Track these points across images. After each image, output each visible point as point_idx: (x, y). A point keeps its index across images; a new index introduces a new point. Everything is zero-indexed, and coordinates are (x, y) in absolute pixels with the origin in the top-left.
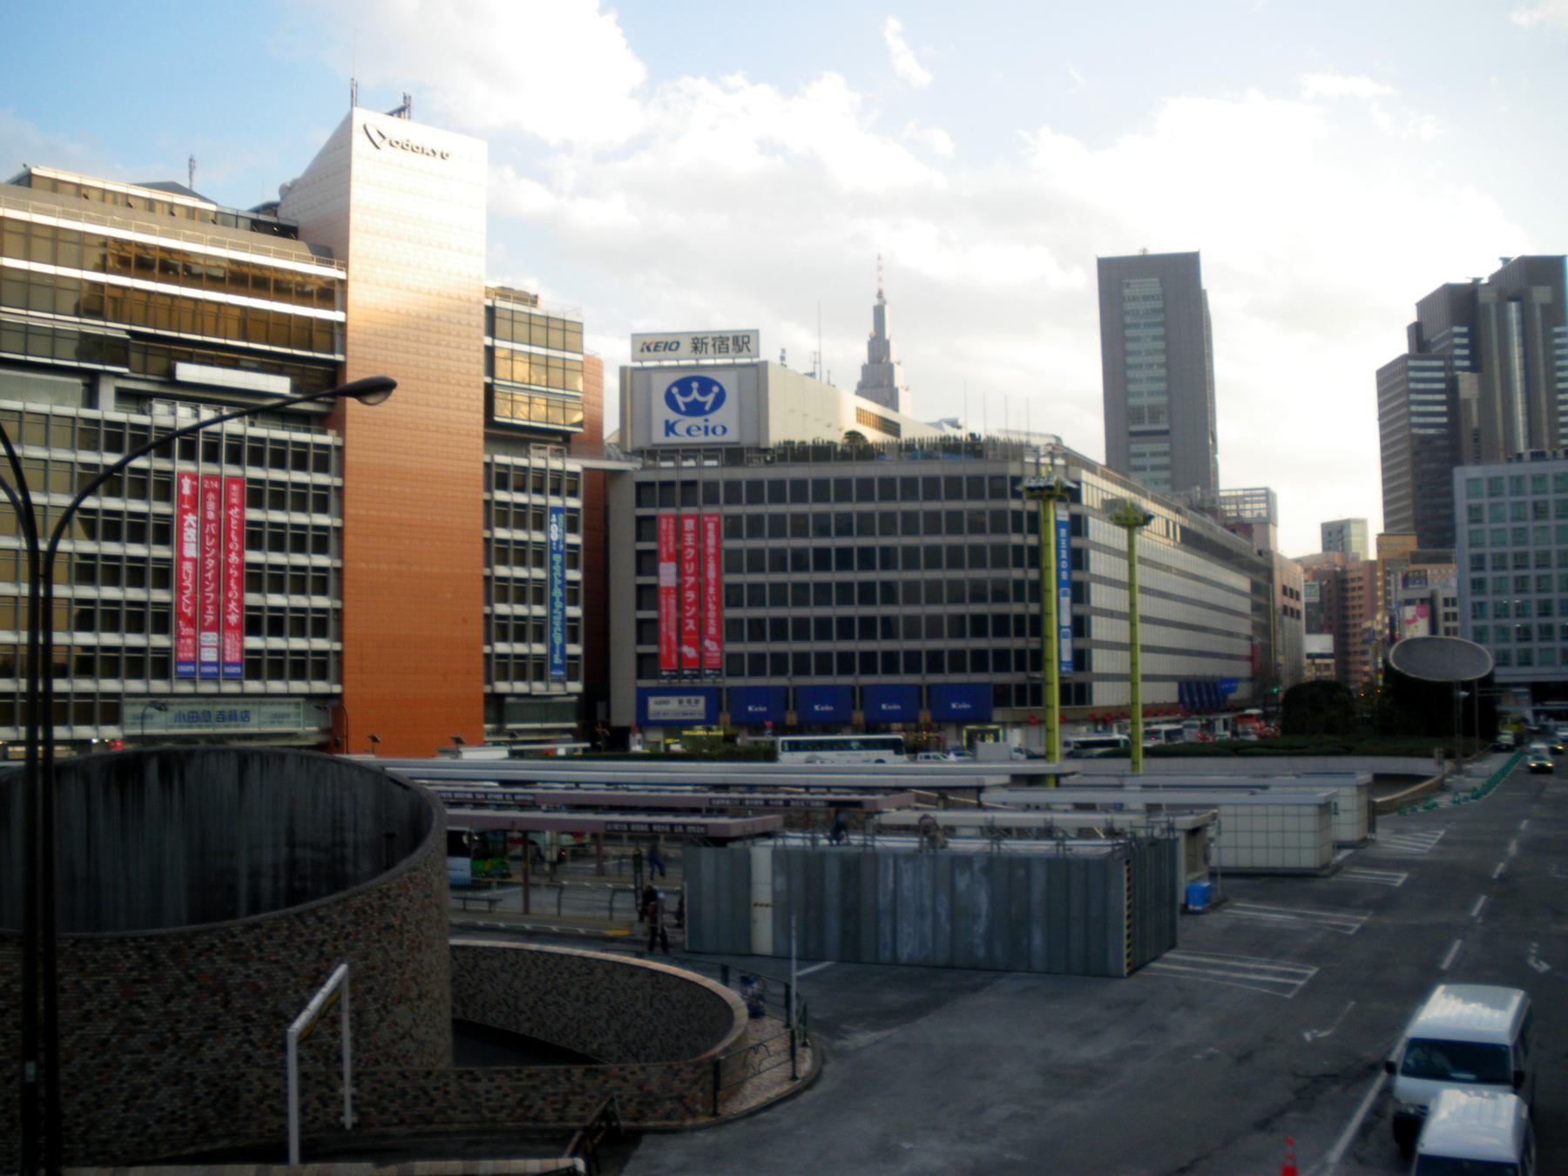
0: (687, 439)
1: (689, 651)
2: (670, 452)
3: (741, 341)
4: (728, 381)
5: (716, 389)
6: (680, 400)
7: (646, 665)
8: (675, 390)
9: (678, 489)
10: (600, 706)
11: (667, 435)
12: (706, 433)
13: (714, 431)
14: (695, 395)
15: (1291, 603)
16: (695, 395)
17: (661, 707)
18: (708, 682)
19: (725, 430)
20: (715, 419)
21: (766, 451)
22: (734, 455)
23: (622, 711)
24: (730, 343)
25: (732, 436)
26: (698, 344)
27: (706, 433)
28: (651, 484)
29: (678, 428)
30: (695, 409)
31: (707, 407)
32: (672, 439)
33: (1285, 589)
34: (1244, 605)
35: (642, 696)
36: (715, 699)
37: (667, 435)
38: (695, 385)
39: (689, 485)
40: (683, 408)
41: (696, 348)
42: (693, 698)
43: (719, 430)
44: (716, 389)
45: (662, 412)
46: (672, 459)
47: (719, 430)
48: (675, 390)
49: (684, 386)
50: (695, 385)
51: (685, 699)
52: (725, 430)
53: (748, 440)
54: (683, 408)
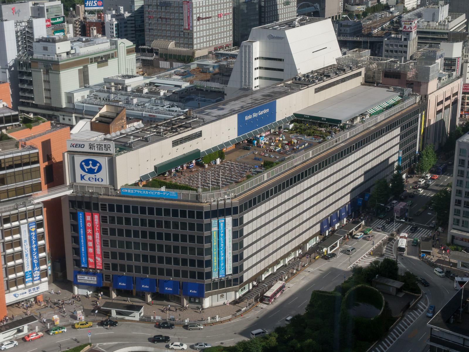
0: (89, 182)
2: (83, 187)
4: (103, 161)
5: (98, 165)
6: (86, 167)
8: (83, 163)
12: (96, 181)
13: (98, 180)
14: (91, 166)
16: (91, 166)
17: (82, 279)
19: (102, 180)
20: (98, 175)
24: (103, 146)
29: (85, 177)
30: (91, 171)
31: (95, 171)
38: (91, 162)
40: (87, 171)
41: (91, 148)
43: (100, 180)
45: (79, 172)
47: (100, 180)
48: (83, 163)
49: (87, 162)
50: (91, 162)
52: (102, 180)
54: (87, 171)
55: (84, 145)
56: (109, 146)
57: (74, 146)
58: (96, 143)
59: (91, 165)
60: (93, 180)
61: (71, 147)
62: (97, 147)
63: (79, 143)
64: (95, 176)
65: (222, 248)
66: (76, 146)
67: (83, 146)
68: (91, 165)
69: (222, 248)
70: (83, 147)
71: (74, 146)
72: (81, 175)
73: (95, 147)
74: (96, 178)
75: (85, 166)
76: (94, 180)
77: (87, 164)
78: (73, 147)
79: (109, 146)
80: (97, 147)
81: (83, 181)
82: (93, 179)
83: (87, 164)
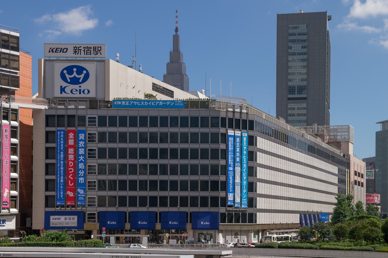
0: (71, 95)
1: (71, 194)
2: (62, 101)
3: (97, 50)
4: (91, 67)
5: (85, 72)
6: (68, 76)
7: (49, 201)
8: (65, 72)
9: (66, 118)
10: (28, 219)
11: (61, 93)
12: (80, 93)
14: (75, 74)
15: (359, 179)
16: (75, 74)
18: (79, 209)
19: (89, 92)
20: (84, 86)
21: (108, 102)
22: (93, 103)
23: (38, 222)
24: (92, 50)
25: (92, 95)
26: (76, 50)
27: (80, 93)
28: (54, 116)
29: (66, 90)
30: (75, 81)
31: (80, 81)
32: (64, 95)
33: (356, 173)
34: (335, 180)
35: (48, 215)
36: (81, 216)
37: (61, 93)
38: (75, 69)
39: (71, 117)
40: (69, 81)
41: (75, 52)
42: (72, 217)
43: (86, 92)
44: (85, 72)
45: (59, 82)
46: (64, 104)
47: (86, 92)
48: (65, 72)
49: (70, 70)
50: (75, 69)
51: (68, 217)
52: (89, 92)
53: (100, 97)
54: (69, 81)
55: (67, 49)
56: (99, 49)
57: (54, 50)
58: (83, 46)
59: (75, 73)
60: (76, 92)
61: (49, 52)
62: (84, 51)
63: (60, 46)
64: (80, 87)
65: (244, 170)
66: (56, 50)
67: (65, 50)
68: (75, 73)
69: (244, 170)
70: (66, 52)
71: (54, 50)
72: (61, 87)
73: (82, 51)
74: (80, 90)
75: (67, 75)
76: (78, 92)
77: (70, 73)
78: (53, 52)
79: (99, 49)
80: (84, 51)
81: (64, 95)
82: (77, 91)
83: (70, 73)
